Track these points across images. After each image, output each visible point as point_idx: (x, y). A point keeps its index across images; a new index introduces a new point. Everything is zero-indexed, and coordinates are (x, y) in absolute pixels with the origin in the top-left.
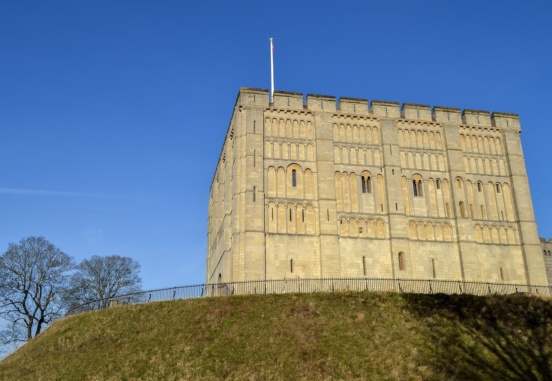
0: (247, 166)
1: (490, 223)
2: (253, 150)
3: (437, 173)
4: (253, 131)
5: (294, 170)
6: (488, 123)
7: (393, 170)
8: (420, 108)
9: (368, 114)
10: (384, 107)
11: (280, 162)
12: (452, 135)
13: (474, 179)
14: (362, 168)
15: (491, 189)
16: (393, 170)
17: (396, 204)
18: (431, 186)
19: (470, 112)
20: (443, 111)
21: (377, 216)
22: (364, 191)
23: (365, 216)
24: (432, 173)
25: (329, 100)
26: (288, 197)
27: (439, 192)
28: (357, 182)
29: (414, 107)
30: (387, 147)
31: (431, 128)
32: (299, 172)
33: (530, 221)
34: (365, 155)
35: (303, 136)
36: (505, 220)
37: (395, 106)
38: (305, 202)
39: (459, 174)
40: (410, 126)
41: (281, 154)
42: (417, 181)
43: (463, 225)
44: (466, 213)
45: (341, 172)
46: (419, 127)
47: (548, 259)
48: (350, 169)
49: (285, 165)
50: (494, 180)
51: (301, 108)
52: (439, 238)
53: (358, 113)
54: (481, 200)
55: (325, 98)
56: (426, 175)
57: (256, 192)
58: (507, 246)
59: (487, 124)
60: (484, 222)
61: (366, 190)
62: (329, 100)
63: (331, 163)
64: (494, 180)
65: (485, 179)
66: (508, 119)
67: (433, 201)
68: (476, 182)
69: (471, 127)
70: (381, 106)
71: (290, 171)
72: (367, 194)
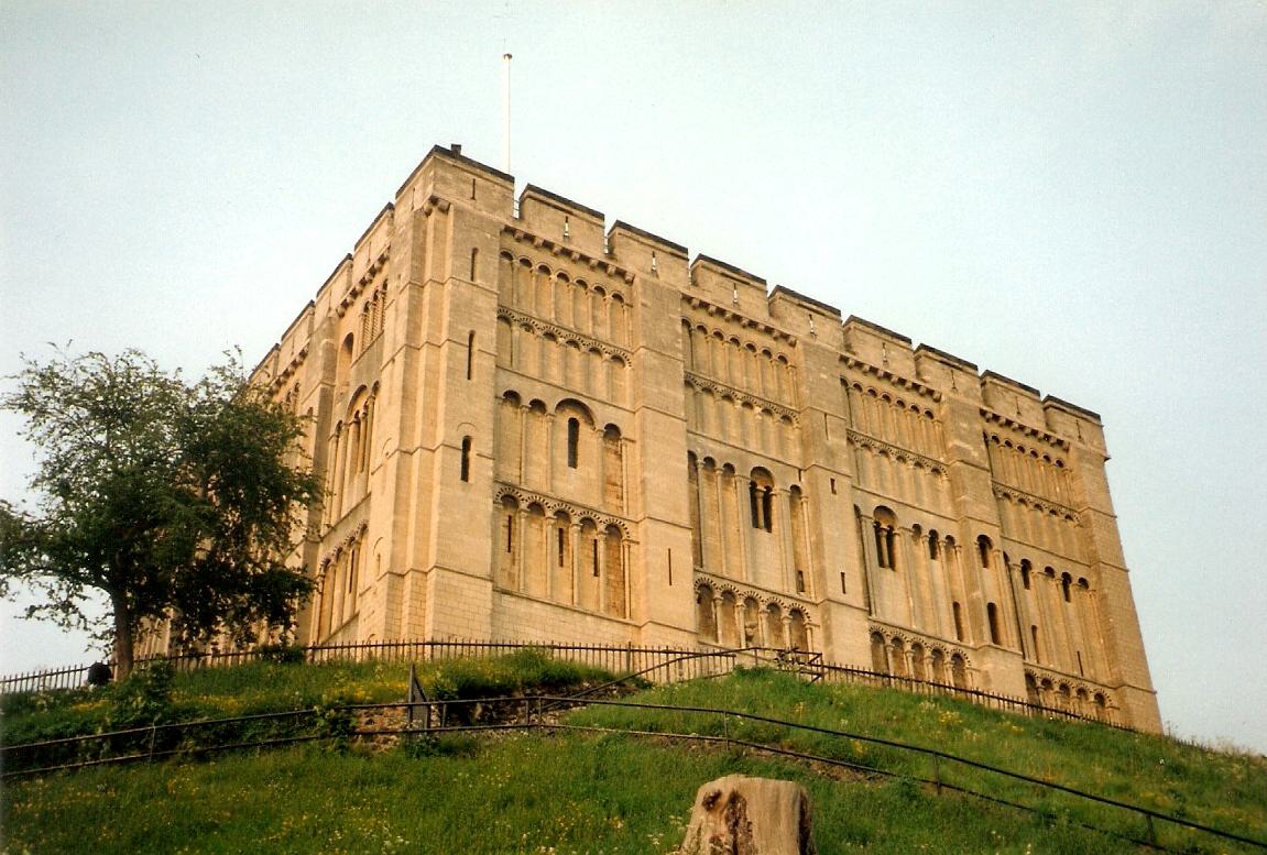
0: (451, 371)
2: (468, 330)
4: (468, 279)
5: (574, 424)
6: (1040, 418)
7: (833, 481)
8: (889, 338)
10: (806, 311)
11: (539, 387)
17: (843, 574)
22: (756, 524)
23: (761, 593)
25: (672, 254)
28: (737, 500)
32: (584, 429)
35: (604, 333)
36: (1087, 676)
41: (543, 368)
44: (1003, 637)
46: (884, 387)
56: (905, 519)
57: (472, 454)
62: (672, 254)
63: (679, 421)
64: (1060, 567)
66: (1081, 422)
71: (564, 421)
72: (763, 533)
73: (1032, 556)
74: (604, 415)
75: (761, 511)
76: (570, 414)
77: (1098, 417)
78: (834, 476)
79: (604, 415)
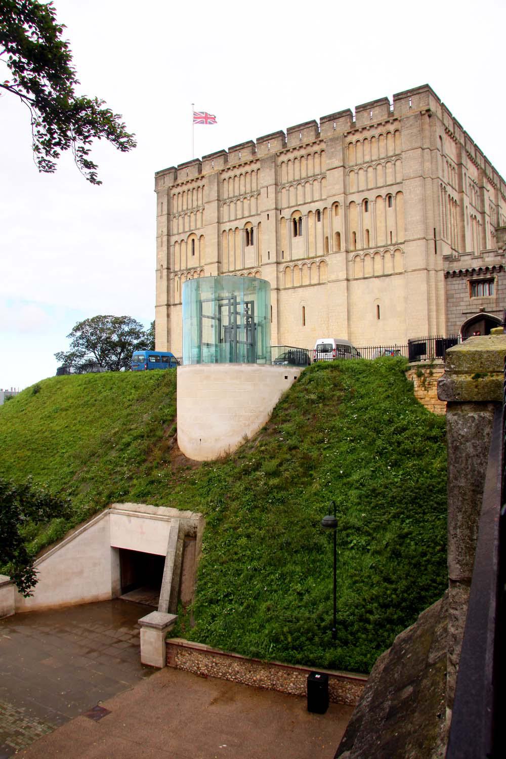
1: (372, 251)
3: (312, 204)
5: (193, 240)
7: (268, 215)
9: (251, 158)
12: (333, 150)
13: (358, 198)
14: (244, 221)
15: (381, 204)
16: (268, 215)
18: (312, 220)
19: (362, 109)
20: (329, 121)
21: (255, 269)
22: (248, 244)
24: (316, 203)
25: (219, 156)
26: (188, 267)
27: (319, 224)
28: (241, 236)
29: (297, 129)
30: (263, 191)
31: (316, 148)
33: (419, 239)
34: (250, 205)
37: (277, 137)
38: (198, 269)
39: (336, 199)
40: (297, 154)
42: (297, 219)
43: (335, 262)
45: (227, 231)
46: (303, 152)
47: (454, 282)
48: (233, 225)
49: (184, 236)
50: (384, 192)
51: (196, 175)
52: (314, 281)
53: (243, 160)
54: (367, 224)
55: (215, 156)
56: (304, 210)
58: (389, 277)
59: (382, 116)
60: (365, 251)
61: (250, 242)
62: (219, 156)
65: (371, 196)
67: (312, 239)
68: (360, 201)
69: (360, 130)
70: (265, 143)
71: (190, 242)
73: (366, 195)
74: (198, 233)
75: (249, 237)
76: (192, 237)
77: (427, 86)
78: (267, 213)
79: (198, 233)
